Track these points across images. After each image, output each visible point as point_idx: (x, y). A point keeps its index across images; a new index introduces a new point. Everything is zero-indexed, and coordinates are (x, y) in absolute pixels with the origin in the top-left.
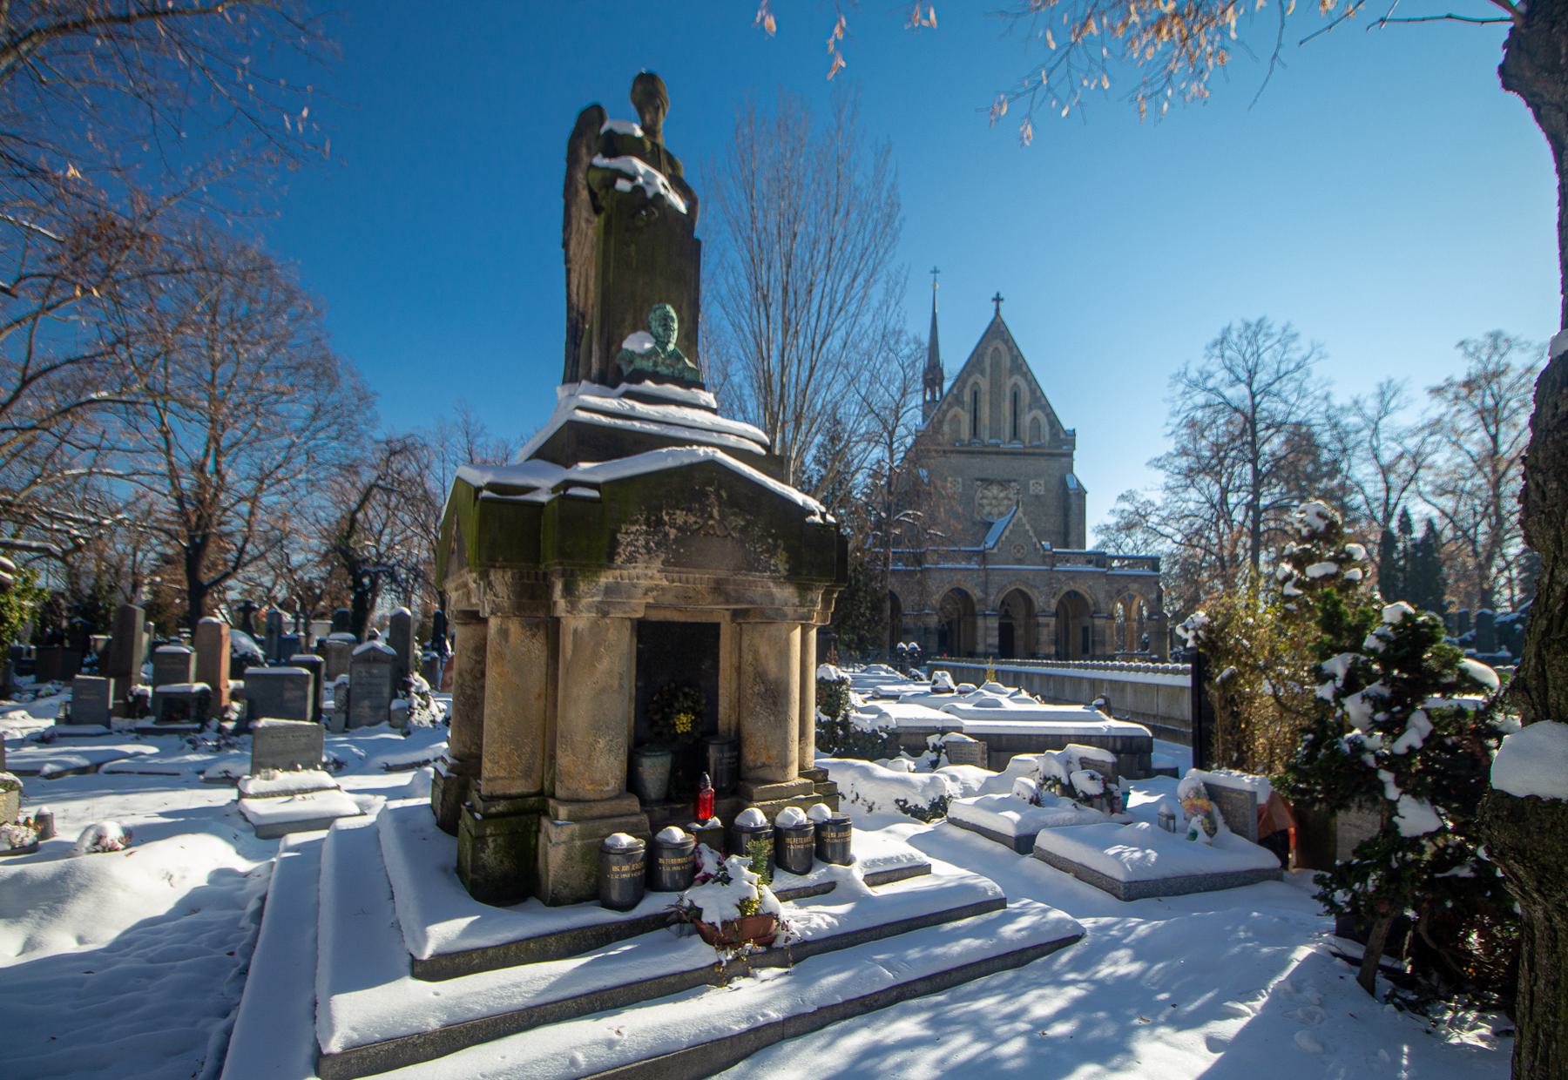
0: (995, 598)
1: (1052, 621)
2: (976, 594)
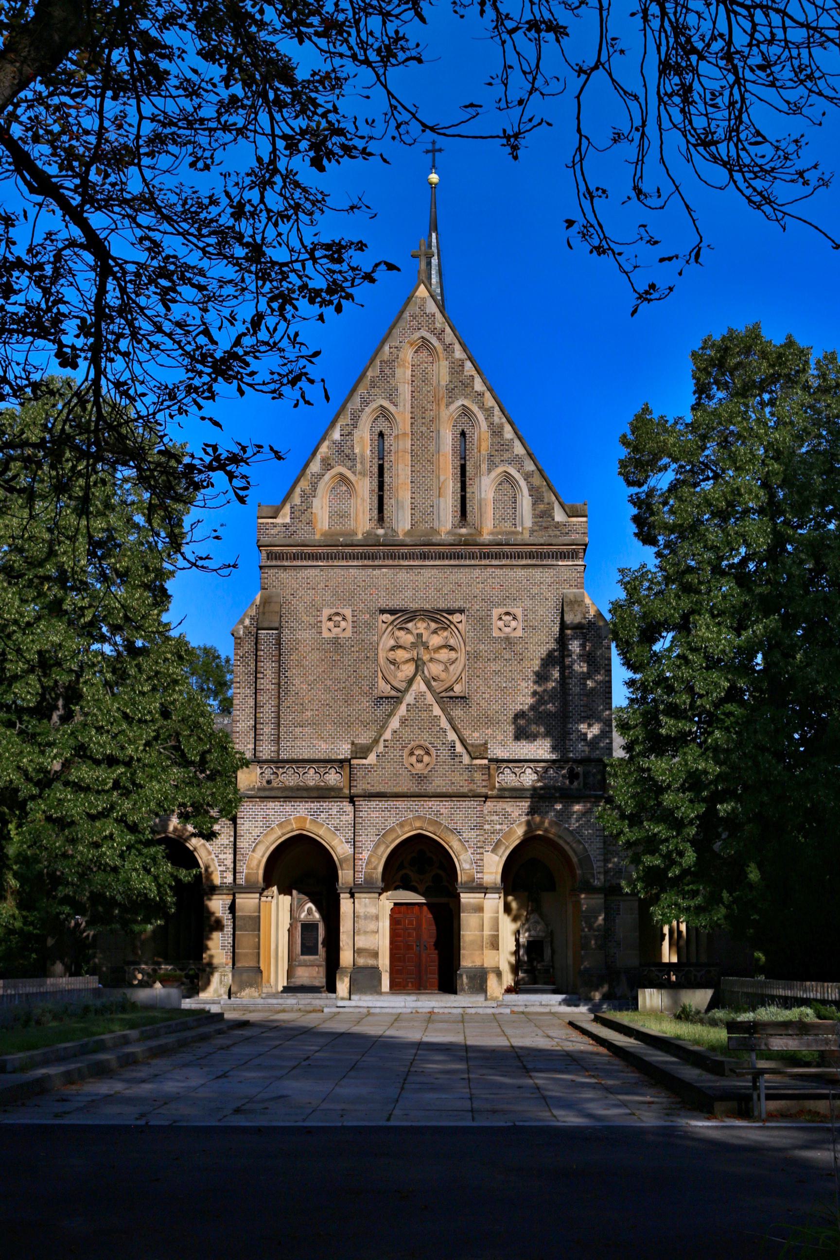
0: (373, 858)
1: (493, 903)
2: (340, 848)
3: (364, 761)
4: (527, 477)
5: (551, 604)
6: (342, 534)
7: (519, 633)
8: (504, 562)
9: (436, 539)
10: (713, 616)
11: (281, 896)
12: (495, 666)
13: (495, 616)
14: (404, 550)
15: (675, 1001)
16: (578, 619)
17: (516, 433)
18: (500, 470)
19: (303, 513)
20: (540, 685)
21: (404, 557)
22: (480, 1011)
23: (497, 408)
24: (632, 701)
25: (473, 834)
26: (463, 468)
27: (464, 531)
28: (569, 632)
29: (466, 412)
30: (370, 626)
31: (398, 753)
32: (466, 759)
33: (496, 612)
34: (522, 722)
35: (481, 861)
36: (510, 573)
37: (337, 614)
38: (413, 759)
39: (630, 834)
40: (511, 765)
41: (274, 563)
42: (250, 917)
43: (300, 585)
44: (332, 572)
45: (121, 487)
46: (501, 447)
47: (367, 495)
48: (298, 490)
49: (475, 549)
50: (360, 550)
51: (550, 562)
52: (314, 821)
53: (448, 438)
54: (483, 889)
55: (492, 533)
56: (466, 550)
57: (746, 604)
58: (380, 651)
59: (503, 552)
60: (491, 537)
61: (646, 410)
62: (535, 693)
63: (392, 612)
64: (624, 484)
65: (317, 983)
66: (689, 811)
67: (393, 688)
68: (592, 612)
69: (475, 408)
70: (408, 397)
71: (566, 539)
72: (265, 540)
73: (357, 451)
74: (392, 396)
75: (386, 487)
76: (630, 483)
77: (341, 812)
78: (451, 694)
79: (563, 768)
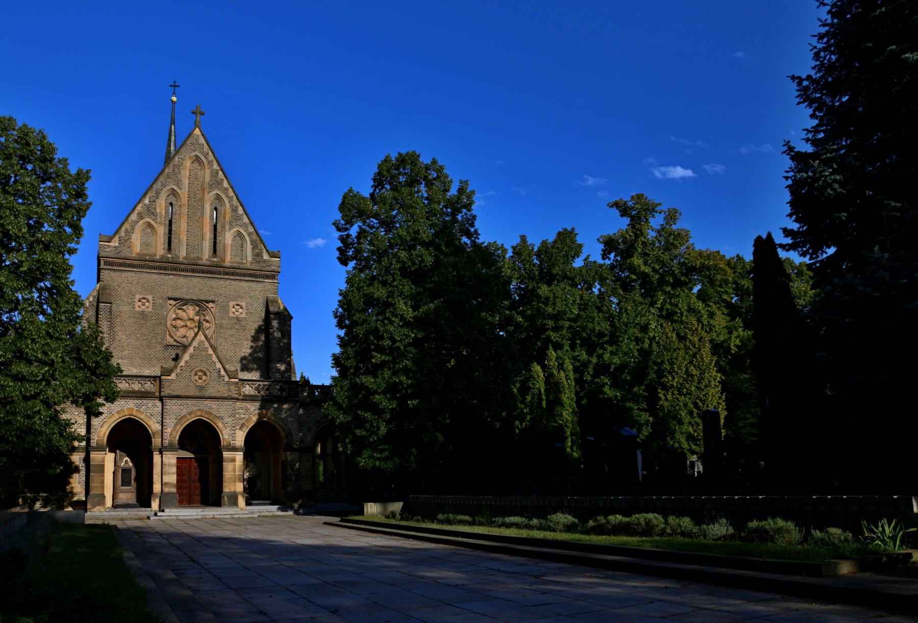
0: (173, 432)
1: (239, 457)
2: (154, 426)
4: (250, 234)
7: (244, 315)
9: (200, 262)
12: (230, 332)
13: (231, 306)
15: (385, 509)
16: (276, 310)
18: (236, 229)
21: (183, 270)
22: (241, 516)
26: (215, 226)
29: (218, 197)
30: (162, 306)
32: (226, 379)
33: (232, 304)
34: (245, 362)
35: (234, 434)
37: (144, 298)
38: (197, 378)
44: (142, 275)
47: (162, 235)
48: (123, 229)
50: (158, 264)
54: (234, 449)
56: (216, 270)
57: (418, 294)
62: (252, 347)
63: (175, 299)
65: (130, 502)
67: (175, 340)
68: (282, 308)
69: (223, 196)
70: (187, 185)
71: (269, 269)
74: (179, 183)
77: (154, 406)
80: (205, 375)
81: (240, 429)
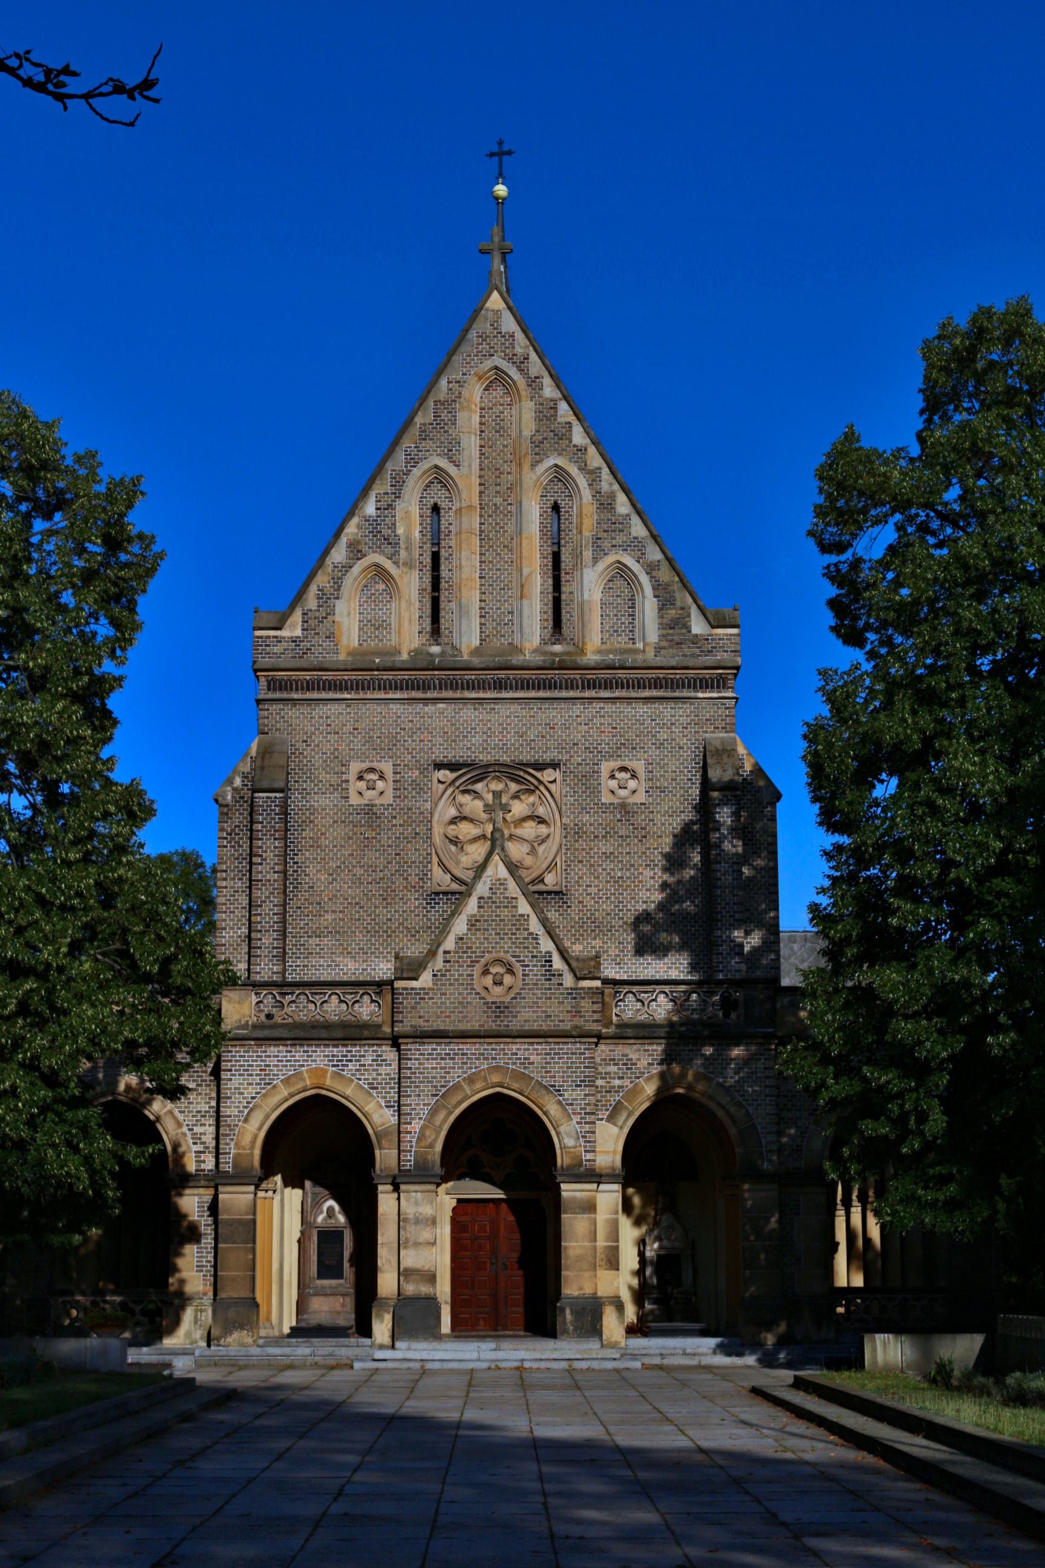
0: (426, 1130)
1: (609, 1196)
2: (377, 1115)
3: (414, 984)
4: (651, 569)
5: (686, 754)
6: (379, 654)
7: (641, 797)
8: (617, 693)
9: (516, 660)
10: (972, 740)
11: (288, 1190)
12: (605, 847)
14: (470, 676)
16: (728, 776)
17: (633, 505)
18: (611, 559)
19: (320, 622)
20: (672, 874)
21: (471, 686)
22: (595, 1365)
23: (605, 470)
24: (835, 880)
25: (579, 1093)
26: (556, 557)
27: (557, 648)
28: (715, 794)
29: (560, 475)
30: (419, 788)
31: (465, 971)
32: (568, 980)
33: (606, 767)
34: (646, 928)
36: (627, 709)
37: (372, 770)
38: (488, 980)
39: (838, 1088)
40: (635, 989)
41: (278, 695)
42: (240, 1221)
43: (318, 728)
44: (363, 708)
45: (39, 547)
46: (611, 525)
48: (313, 589)
49: (575, 675)
50: (405, 675)
51: (685, 693)
52: (337, 1075)
53: (533, 512)
54: (595, 1176)
55: (599, 652)
56: (561, 676)
58: (435, 824)
59: (614, 679)
60: (598, 657)
61: (850, 436)
62: (664, 886)
63: (452, 767)
64: (816, 550)
65: (341, 1322)
66: (936, 1046)
67: (455, 878)
68: (748, 767)
69: (573, 470)
71: (708, 660)
72: (264, 661)
73: (400, 531)
74: (452, 452)
75: (443, 585)
76: (825, 548)
77: (379, 1060)
78: (541, 887)
79: (714, 993)
80: (510, 971)
81: (611, 1119)
